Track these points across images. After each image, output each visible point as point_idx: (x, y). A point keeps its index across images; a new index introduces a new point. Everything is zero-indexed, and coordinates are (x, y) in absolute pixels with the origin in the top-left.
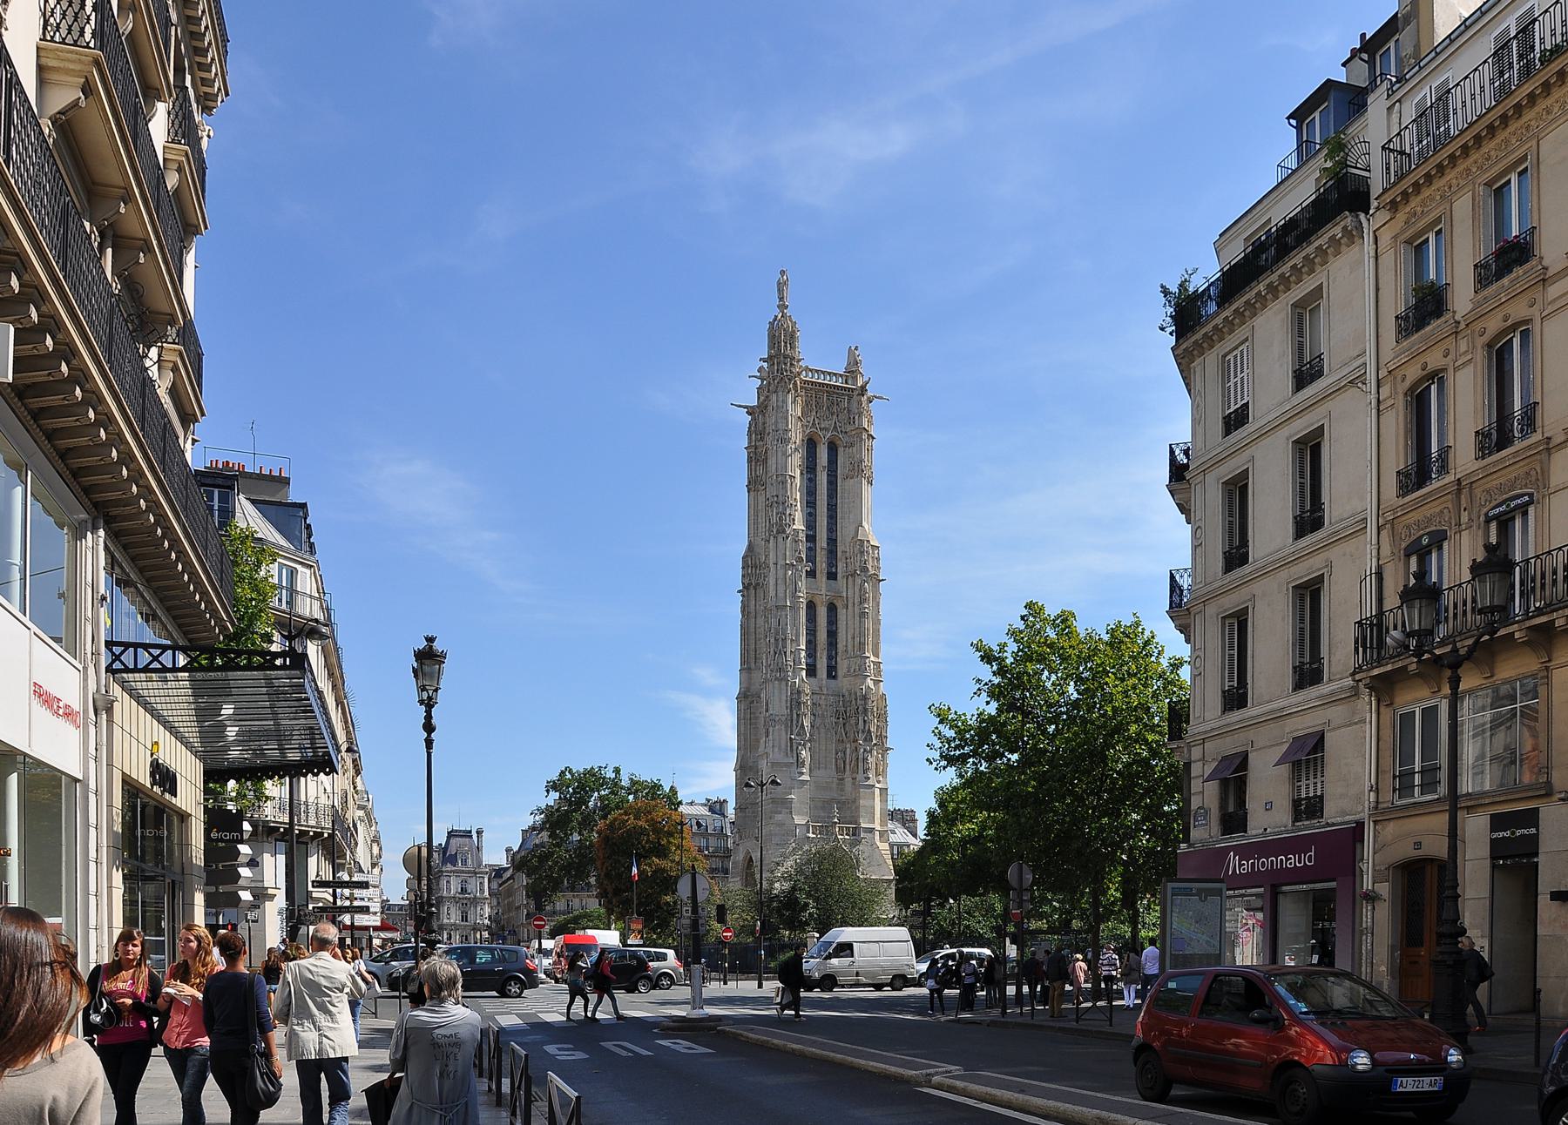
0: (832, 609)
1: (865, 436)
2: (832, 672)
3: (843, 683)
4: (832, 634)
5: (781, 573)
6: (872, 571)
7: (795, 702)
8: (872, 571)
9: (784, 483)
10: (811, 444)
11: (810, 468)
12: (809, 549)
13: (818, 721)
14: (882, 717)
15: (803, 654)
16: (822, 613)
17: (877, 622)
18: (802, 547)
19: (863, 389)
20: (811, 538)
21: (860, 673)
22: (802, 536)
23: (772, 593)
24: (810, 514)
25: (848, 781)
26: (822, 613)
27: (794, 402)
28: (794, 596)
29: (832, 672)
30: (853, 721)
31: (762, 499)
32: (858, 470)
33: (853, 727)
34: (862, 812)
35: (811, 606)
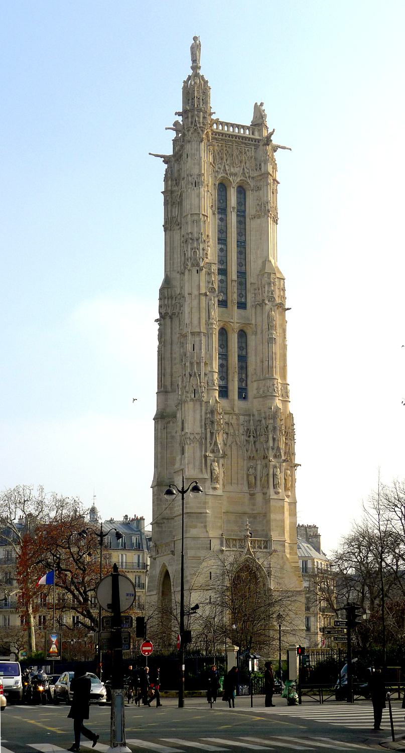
0: (242, 334)
1: (270, 180)
2: (243, 394)
3: (254, 404)
4: (243, 359)
5: (195, 303)
6: (278, 301)
8: (278, 301)
9: (198, 221)
10: (222, 188)
11: (222, 210)
12: (221, 281)
14: (290, 435)
15: (216, 376)
16: (234, 340)
17: (284, 347)
18: (216, 278)
19: (268, 140)
20: (223, 272)
22: (215, 268)
24: (221, 250)
26: (234, 340)
28: (209, 324)
29: (243, 394)
30: (263, 439)
31: (177, 237)
33: (264, 443)
35: (223, 332)
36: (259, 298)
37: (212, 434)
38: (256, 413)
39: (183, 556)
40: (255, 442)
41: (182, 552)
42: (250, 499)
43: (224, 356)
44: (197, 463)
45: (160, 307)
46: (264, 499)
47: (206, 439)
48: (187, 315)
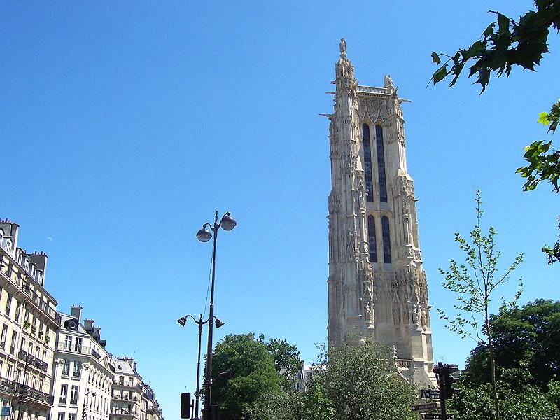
0: (385, 220)
2: (388, 259)
3: (396, 263)
4: (386, 234)
5: (349, 197)
7: (362, 276)
9: (349, 144)
13: (380, 289)
14: (423, 285)
15: (366, 246)
17: (415, 226)
19: (394, 95)
20: (369, 178)
21: (406, 255)
22: (362, 175)
23: (344, 209)
25: (403, 329)
27: (353, 103)
29: (388, 259)
32: (395, 137)
33: (403, 294)
34: (414, 350)
35: (371, 219)
36: (395, 194)
37: (364, 285)
38: (398, 272)
39: (212, 307)
40: (398, 292)
41: (212, 303)
42: (396, 332)
43: (372, 233)
44: (355, 306)
45: (329, 207)
46: (407, 331)
47: (360, 289)
48: (344, 206)
